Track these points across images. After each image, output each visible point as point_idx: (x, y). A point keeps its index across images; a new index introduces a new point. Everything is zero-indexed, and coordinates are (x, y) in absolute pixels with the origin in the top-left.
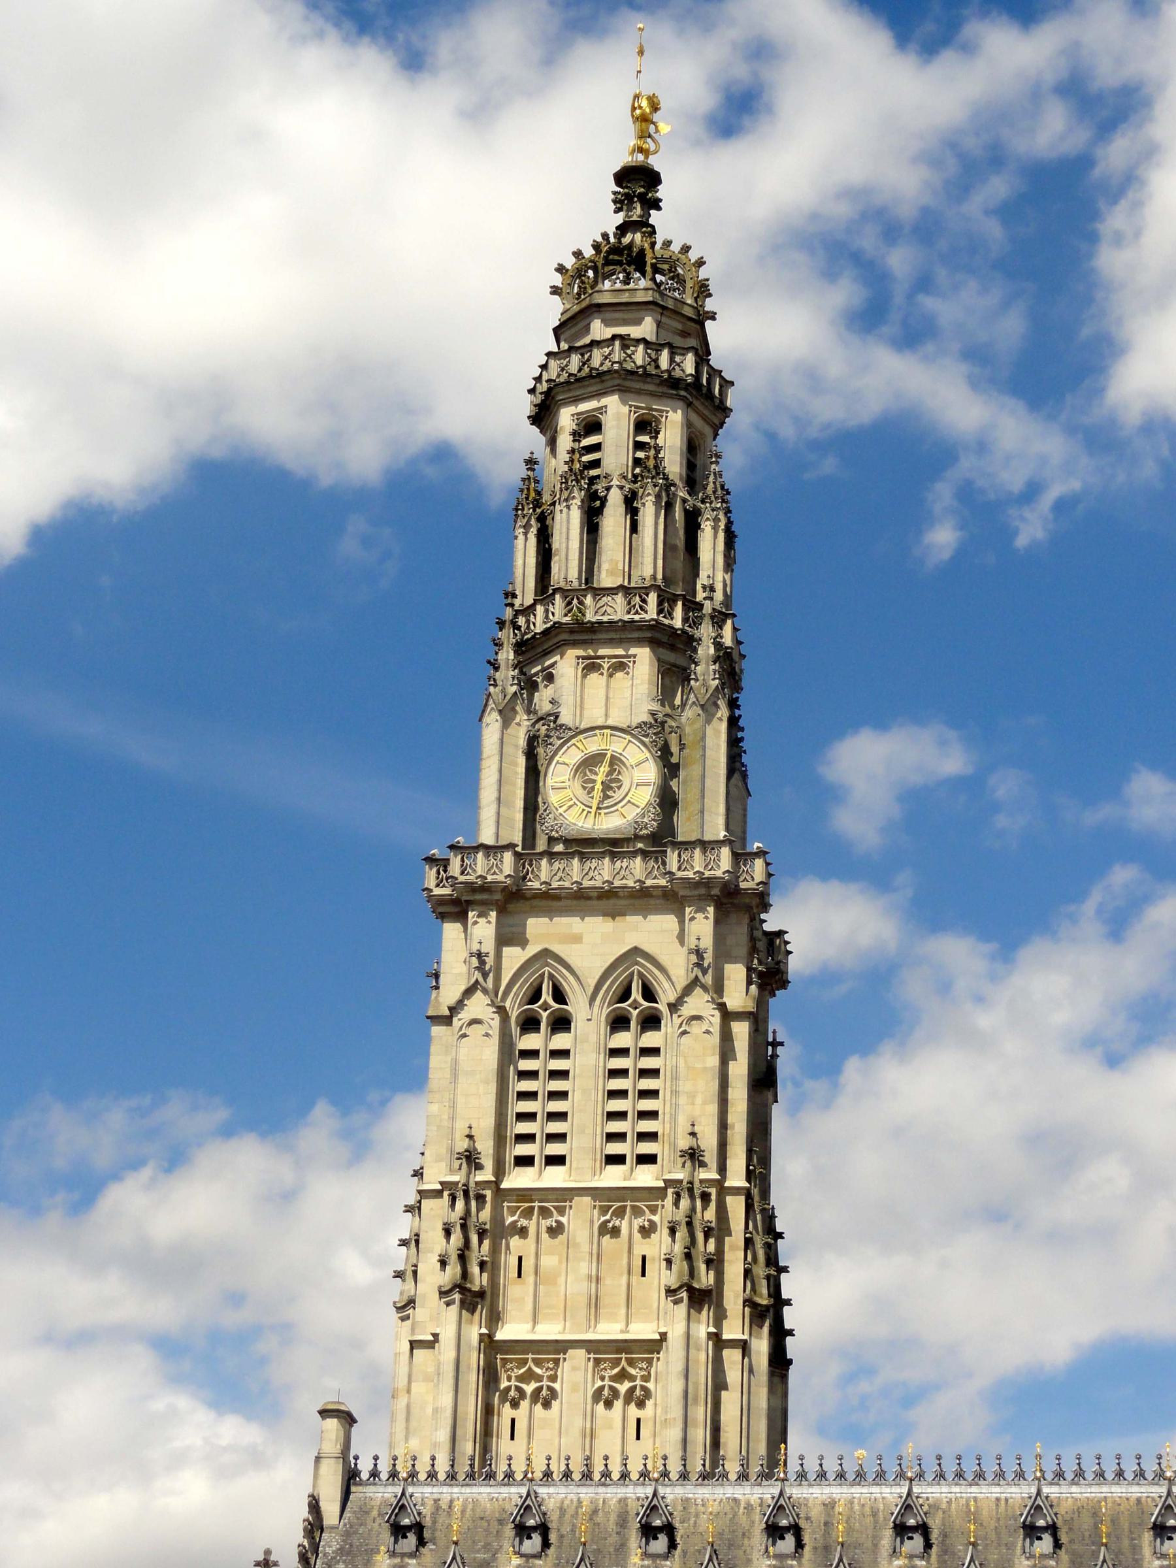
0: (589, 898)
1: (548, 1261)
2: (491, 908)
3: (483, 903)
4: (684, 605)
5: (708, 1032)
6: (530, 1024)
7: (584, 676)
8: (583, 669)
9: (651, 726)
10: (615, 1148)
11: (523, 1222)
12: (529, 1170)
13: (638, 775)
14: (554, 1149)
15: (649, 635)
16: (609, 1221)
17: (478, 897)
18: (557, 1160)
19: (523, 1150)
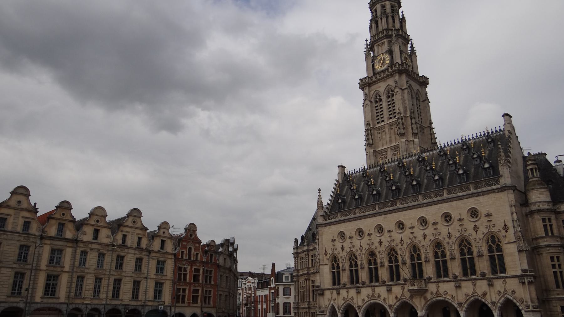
1: (384, 137)
5: (399, 93)
6: (376, 102)
7: (378, 47)
9: (388, 50)
10: (391, 116)
11: (379, 132)
12: (379, 124)
13: (387, 59)
14: (382, 119)
17: (365, 86)
18: (383, 121)
19: (378, 121)
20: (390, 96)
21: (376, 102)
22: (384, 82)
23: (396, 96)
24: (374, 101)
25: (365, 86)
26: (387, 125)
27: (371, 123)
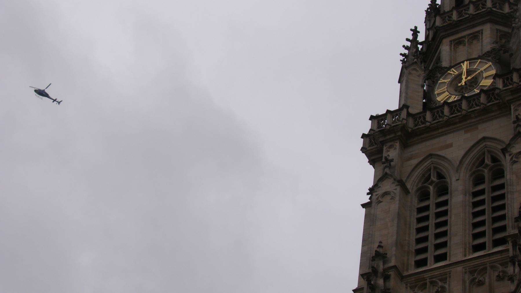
0: (455, 123)
2: (396, 142)
3: (391, 140)
4: (510, 7)
8: (454, 45)
15: (488, 17)
16: (475, 279)
17: (388, 137)
20: (483, 178)
21: (424, 195)
22: (466, 132)
23: (514, 166)
24: (415, 189)
25: (388, 137)
26: (459, 269)
27: (392, 253)
